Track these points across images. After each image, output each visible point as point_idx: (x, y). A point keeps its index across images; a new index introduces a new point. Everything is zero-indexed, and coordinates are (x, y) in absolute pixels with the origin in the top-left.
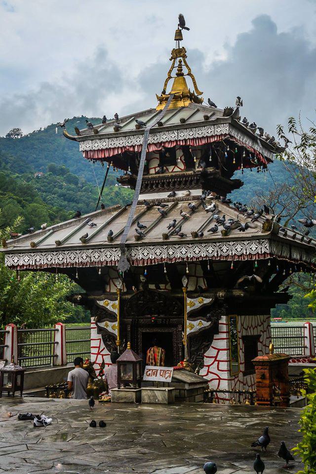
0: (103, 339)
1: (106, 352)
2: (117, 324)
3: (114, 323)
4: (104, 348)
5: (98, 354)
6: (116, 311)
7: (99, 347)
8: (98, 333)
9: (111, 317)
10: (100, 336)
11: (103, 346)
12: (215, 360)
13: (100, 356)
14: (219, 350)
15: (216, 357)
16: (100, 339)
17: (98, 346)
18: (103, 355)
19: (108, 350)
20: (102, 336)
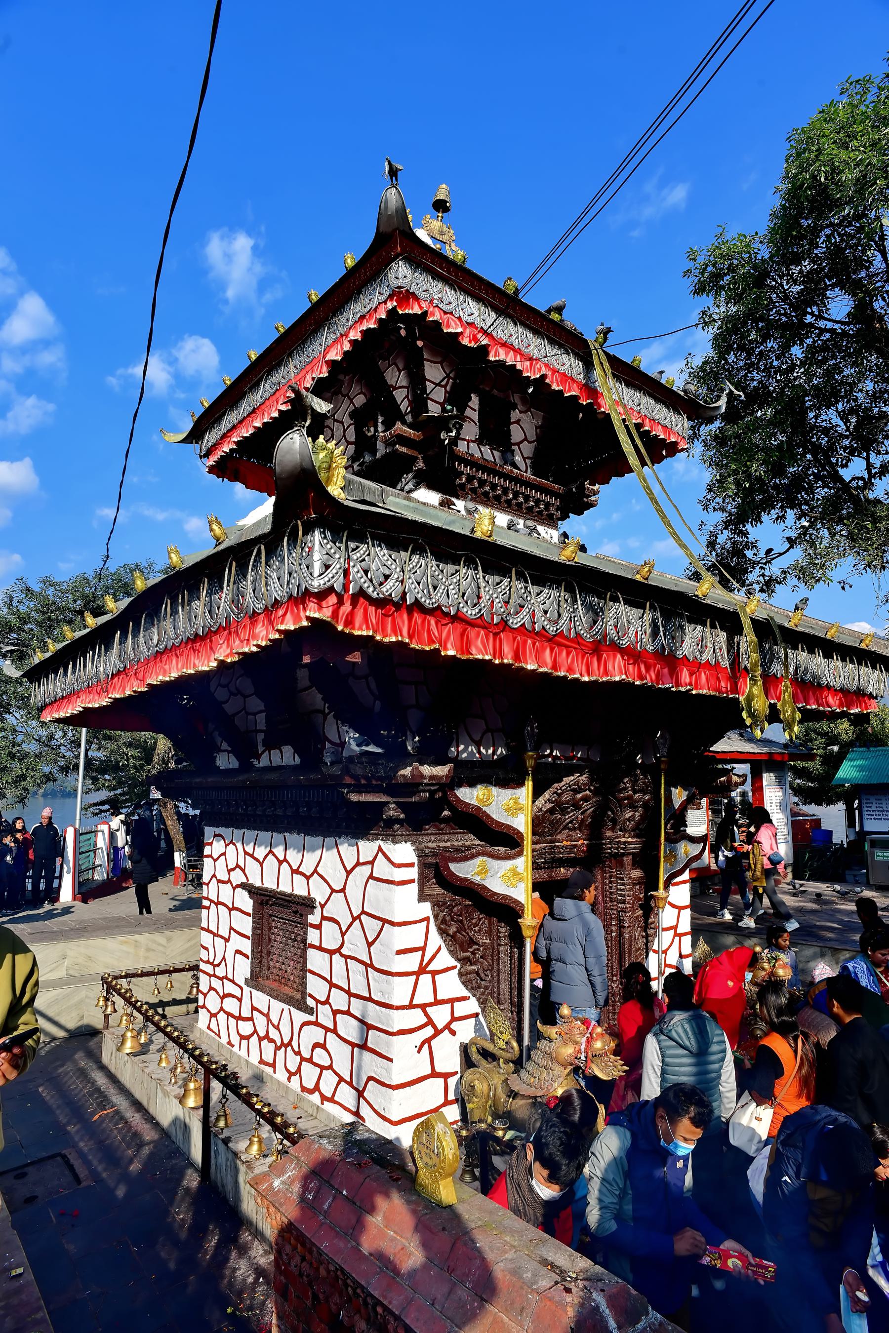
0: (436, 917)
1: (445, 959)
2: (523, 864)
3: (508, 864)
4: (439, 949)
5: (422, 970)
6: (522, 823)
7: (423, 949)
8: (422, 898)
9: (504, 840)
10: (426, 909)
11: (436, 940)
12: (676, 935)
13: (425, 979)
14: (680, 908)
15: (675, 928)
16: (427, 919)
17: (422, 945)
18: (434, 973)
19: (451, 952)
20: (433, 907)
